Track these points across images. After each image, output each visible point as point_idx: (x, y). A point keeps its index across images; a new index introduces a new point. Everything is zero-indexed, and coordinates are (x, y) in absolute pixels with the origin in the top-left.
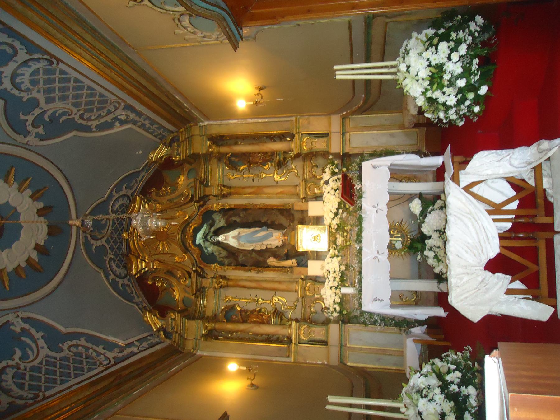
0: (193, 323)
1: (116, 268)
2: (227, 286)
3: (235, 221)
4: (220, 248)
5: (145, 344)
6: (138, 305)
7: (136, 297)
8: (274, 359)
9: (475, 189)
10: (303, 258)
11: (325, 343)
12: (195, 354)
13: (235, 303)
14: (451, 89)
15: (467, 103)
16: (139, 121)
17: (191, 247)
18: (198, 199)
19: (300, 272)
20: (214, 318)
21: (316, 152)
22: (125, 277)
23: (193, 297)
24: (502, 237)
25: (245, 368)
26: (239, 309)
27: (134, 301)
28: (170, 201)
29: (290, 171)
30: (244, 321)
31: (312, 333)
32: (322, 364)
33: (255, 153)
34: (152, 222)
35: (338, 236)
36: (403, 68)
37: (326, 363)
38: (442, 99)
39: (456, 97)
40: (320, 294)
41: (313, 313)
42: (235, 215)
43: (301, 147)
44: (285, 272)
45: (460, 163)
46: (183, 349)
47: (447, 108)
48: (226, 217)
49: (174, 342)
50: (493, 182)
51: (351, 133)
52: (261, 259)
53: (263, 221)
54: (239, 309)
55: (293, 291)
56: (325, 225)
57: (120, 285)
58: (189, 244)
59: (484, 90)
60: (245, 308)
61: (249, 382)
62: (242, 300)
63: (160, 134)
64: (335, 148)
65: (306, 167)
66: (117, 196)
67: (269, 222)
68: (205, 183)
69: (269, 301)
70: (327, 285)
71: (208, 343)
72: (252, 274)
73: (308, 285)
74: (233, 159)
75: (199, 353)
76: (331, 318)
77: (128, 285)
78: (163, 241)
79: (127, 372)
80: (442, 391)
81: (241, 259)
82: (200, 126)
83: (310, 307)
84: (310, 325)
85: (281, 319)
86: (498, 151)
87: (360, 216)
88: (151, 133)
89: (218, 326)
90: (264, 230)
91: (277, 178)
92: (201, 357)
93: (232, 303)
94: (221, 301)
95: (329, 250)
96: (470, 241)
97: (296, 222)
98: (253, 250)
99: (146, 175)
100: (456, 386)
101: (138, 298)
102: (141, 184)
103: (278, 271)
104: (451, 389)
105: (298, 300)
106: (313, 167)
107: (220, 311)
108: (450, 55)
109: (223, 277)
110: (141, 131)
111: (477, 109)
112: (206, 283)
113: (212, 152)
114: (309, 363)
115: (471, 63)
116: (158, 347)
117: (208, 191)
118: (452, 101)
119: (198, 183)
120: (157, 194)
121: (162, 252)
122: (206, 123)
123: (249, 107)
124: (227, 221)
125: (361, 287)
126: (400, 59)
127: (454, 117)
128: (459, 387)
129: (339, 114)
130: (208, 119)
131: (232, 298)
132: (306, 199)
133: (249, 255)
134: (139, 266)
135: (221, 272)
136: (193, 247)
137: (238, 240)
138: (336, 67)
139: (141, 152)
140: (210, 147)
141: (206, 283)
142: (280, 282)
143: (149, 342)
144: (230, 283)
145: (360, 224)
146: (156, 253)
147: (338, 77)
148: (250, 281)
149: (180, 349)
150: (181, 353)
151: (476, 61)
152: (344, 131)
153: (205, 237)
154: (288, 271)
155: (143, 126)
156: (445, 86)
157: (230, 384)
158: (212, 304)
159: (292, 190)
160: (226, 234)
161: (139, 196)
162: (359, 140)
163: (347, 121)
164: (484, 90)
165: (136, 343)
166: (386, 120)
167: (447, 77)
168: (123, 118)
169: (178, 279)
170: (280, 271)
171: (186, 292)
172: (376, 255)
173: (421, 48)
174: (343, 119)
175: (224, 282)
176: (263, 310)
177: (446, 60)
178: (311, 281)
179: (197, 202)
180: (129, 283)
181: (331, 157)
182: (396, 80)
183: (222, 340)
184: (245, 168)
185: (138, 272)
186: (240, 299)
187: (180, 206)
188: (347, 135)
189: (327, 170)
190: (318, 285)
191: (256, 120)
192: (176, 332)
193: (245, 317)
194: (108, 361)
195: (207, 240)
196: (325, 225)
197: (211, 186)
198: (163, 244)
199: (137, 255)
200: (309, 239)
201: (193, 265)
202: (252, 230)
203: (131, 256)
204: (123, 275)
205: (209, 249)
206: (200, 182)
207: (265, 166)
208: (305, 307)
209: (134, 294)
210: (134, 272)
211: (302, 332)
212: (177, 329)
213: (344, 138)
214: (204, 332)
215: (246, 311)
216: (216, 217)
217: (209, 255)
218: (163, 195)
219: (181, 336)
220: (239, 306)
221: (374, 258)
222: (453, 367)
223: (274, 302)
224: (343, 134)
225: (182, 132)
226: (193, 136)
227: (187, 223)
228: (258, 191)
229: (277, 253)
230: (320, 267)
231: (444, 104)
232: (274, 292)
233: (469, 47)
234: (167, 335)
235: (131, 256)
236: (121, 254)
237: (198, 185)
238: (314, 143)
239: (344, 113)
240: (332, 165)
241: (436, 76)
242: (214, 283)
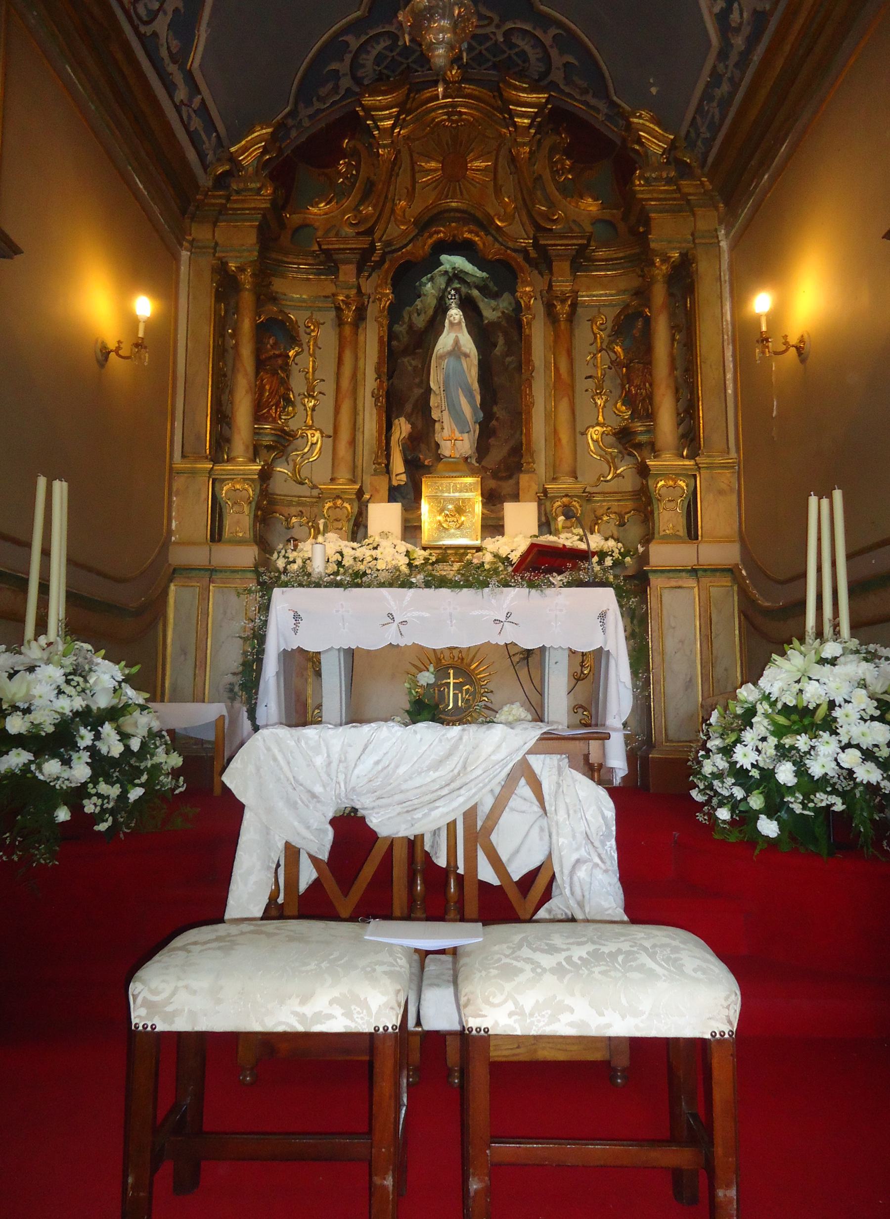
0: (251, 239)
1: (374, 52)
2: (340, 322)
3: (495, 345)
4: (431, 312)
5: (196, 123)
6: (292, 114)
7: (310, 111)
8: (178, 424)
9: (524, 789)
10: (408, 496)
11: (216, 535)
12: (181, 245)
13: (305, 346)
14: (772, 752)
15: (739, 793)
16: (727, 67)
17: (430, 236)
18: (542, 242)
19: (377, 491)
20: (265, 296)
21: (652, 512)
22: (357, 81)
23: (316, 248)
24: (413, 844)
25: (141, 335)
26: (291, 353)
27: (301, 105)
28: (539, 178)
29: (612, 463)
30: (260, 364)
31: (236, 508)
32: (170, 533)
33: (651, 375)
34: (442, 30)
35: (457, 566)
36: (831, 649)
37: (173, 539)
38: (749, 736)
39: (753, 765)
40: (326, 530)
41: (288, 518)
42: (508, 342)
43: (666, 476)
44: (377, 457)
45: (586, 757)
46: (193, 218)
47: (727, 751)
48: (504, 323)
49: (206, 195)
50: (542, 829)
51: (696, 590)
52: (408, 408)
53: (495, 409)
54: (291, 353)
55: (333, 473)
56: (483, 538)
57: (334, 66)
58: (438, 232)
59: (768, 827)
60: (294, 369)
61: (112, 345)
62: (313, 363)
63: (698, 135)
64: (661, 554)
65: (619, 500)
66: (547, 40)
67: (494, 422)
68: (580, 260)
70: (347, 547)
71: (207, 274)
72: (370, 382)
73: (346, 505)
74: (640, 324)
75: (185, 254)
76: (275, 555)
77: (336, 88)
78: (443, 168)
79: (119, 56)
80: (76, 714)
81: (409, 363)
82: (716, 230)
83: (301, 514)
84: (254, 504)
85: (269, 448)
86: (613, 842)
87: (486, 585)
88: (699, 109)
89: (247, 299)
90: (475, 412)
91: (595, 433)
92: (176, 258)
93: (304, 338)
94: (308, 314)
95: (425, 549)
96: (401, 770)
97: (492, 484)
98: (429, 390)
99: (601, 117)
100: (90, 743)
101: (310, 117)
102: (577, 106)
103: (379, 440)
104: (83, 731)
106: (621, 516)
107: (287, 311)
108: (858, 747)
109: (361, 315)
110: (705, 77)
111: (723, 814)
112: (347, 273)
113: (653, 264)
114: (170, 502)
115: (835, 792)
116: (191, 155)
117: (562, 267)
118: (744, 757)
119: (580, 242)
120: (553, 150)
121: (417, 168)
122: (724, 244)
123: (757, 320)
124: (492, 324)
125: (326, 587)
126: (854, 643)
127: (708, 768)
128: (87, 748)
129: (742, 560)
130: (732, 248)
131: (316, 338)
132: (543, 498)
133: (417, 380)
134: (383, 112)
135: (372, 310)
136: (430, 241)
137: (450, 353)
138: (838, 495)
139: (654, 90)
140: (666, 259)
141: (347, 273)
142: (353, 442)
143: (202, 133)
144: (347, 330)
145: (468, 585)
146: (415, 155)
147: (813, 500)
149: (192, 208)
150: (183, 213)
151: (839, 806)
152: (700, 573)
153: (457, 276)
154: (380, 464)
155: (716, 78)
156: (780, 738)
157: (107, 303)
158: (300, 291)
159: (566, 466)
160: (464, 325)
161: (548, 100)
162: (679, 611)
163: (726, 581)
164: (768, 827)
165: (197, 101)
166: (726, 670)
167: (802, 742)
168: (735, 16)
169: (356, 209)
171: (327, 231)
172: (398, 619)
173: (878, 688)
174: (730, 570)
175: (349, 316)
176: (290, 409)
177: (845, 741)
178: (356, 510)
179: (536, 245)
180: (342, 92)
181: (641, 549)
182: (802, 640)
183: (217, 312)
184: (620, 357)
185: (367, 109)
187: (526, 205)
188: (691, 583)
189: (611, 543)
190: (347, 527)
191: (730, 365)
192: (228, 199)
193: (272, 367)
194: (145, 18)
195: (449, 282)
196: (483, 538)
197: (575, 277)
198: (435, 170)
199: (408, 106)
200: (451, 510)
201: (389, 243)
202: (476, 386)
203: (404, 90)
204: (360, 73)
205: (429, 285)
206: (583, 248)
207: (623, 404)
208: (299, 504)
209: (318, 105)
210: (368, 100)
211: (238, 486)
212: (236, 201)
213: (684, 574)
214: (232, 266)
215: (285, 367)
216: (505, 303)
217: (415, 288)
218: (553, 164)
219: (220, 213)
220: (297, 354)
221: (391, 616)
222: (135, 744)
223: (309, 433)
224: (694, 572)
225: (702, 183)
226: (694, 215)
227: (484, 225)
228: (563, 387)
229: (423, 446)
230: (386, 530)
231: (739, 741)
232: (331, 433)
233: (872, 789)
234: (221, 182)
235: (404, 90)
236: (408, 67)
237: (575, 242)
238: (672, 505)
239: (744, 572)
240: (620, 553)
241: (806, 722)
242: (346, 292)
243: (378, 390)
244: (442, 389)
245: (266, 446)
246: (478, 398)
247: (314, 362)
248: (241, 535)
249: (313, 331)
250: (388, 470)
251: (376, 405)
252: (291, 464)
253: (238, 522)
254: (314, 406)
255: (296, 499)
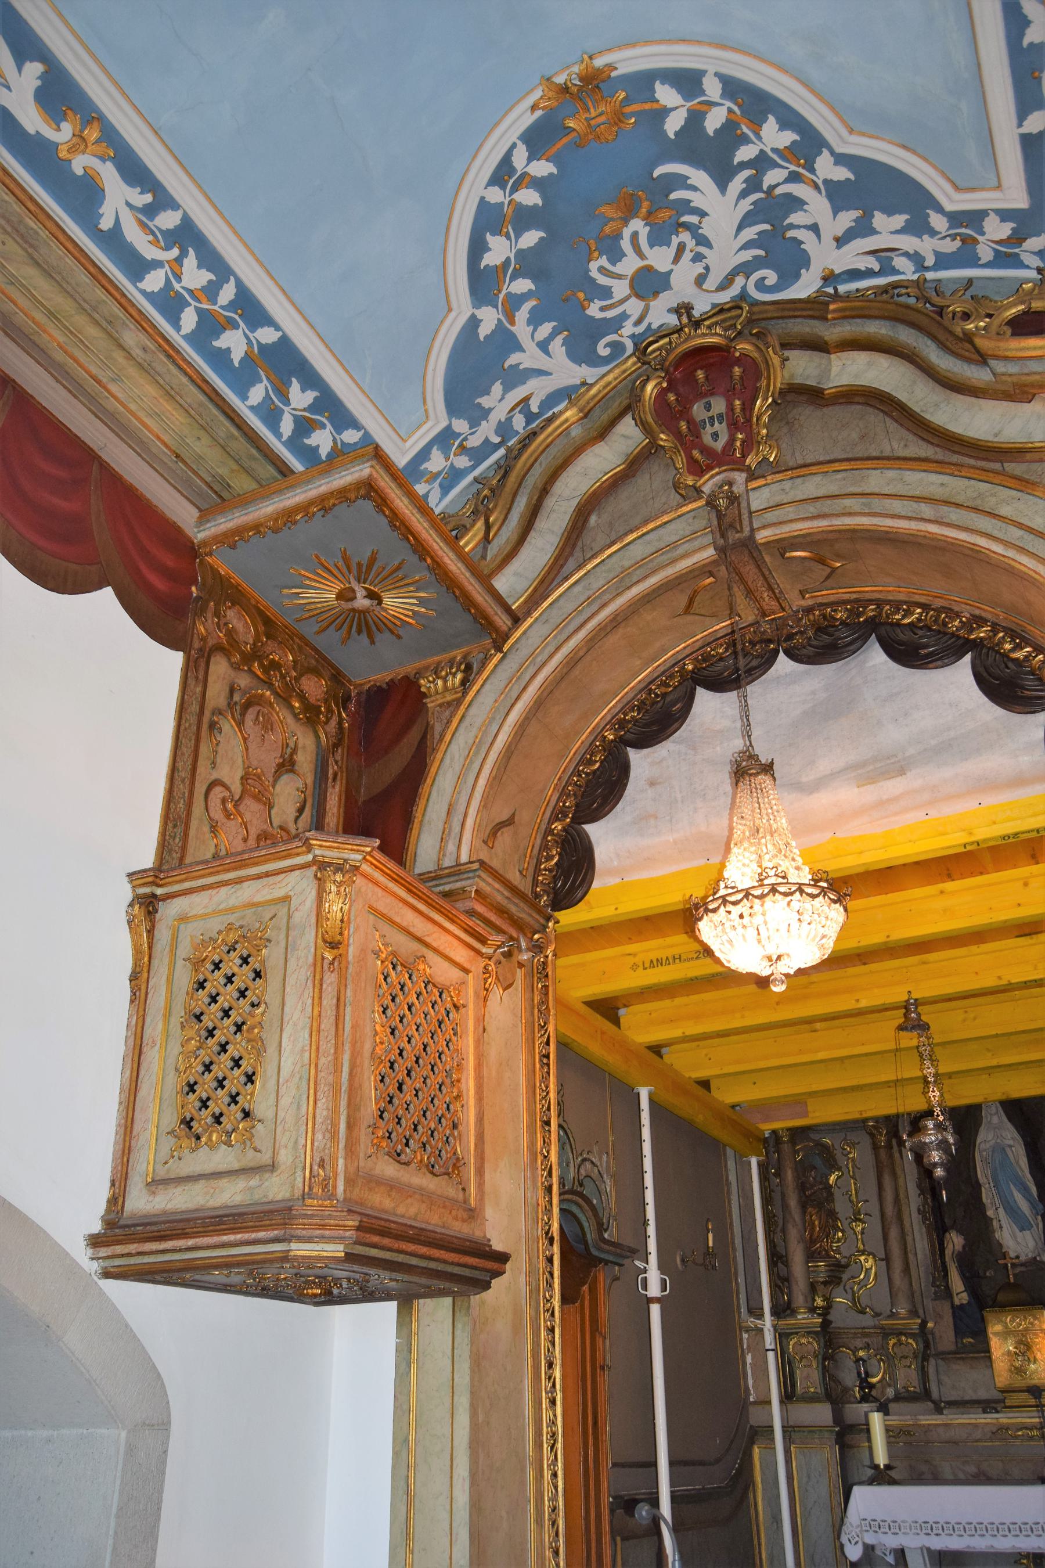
2: (875, 1147)
26: (832, 1179)
69: (861, 1247)
73: (910, 1341)
83: (867, 1347)
84: (820, 1357)
85: (825, 1283)
90: (1033, 1206)
93: (842, 1161)
103: (934, 1261)
105: (877, 1315)
142: (907, 1269)
144: (883, 1153)
148: (897, 1200)
170: (935, 1268)
186: (854, 1177)
211: (803, 1341)
220: (839, 1177)
243: (924, 1207)
244: (992, 1185)
245: (822, 1283)
246: (1034, 1190)
247: (855, 1184)
248: (812, 1390)
249: (850, 1153)
250: (948, 1294)
251: (924, 1223)
252: (849, 1291)
253: (808, 1377)
254: (863, 1229)
255: (860, 1331)
